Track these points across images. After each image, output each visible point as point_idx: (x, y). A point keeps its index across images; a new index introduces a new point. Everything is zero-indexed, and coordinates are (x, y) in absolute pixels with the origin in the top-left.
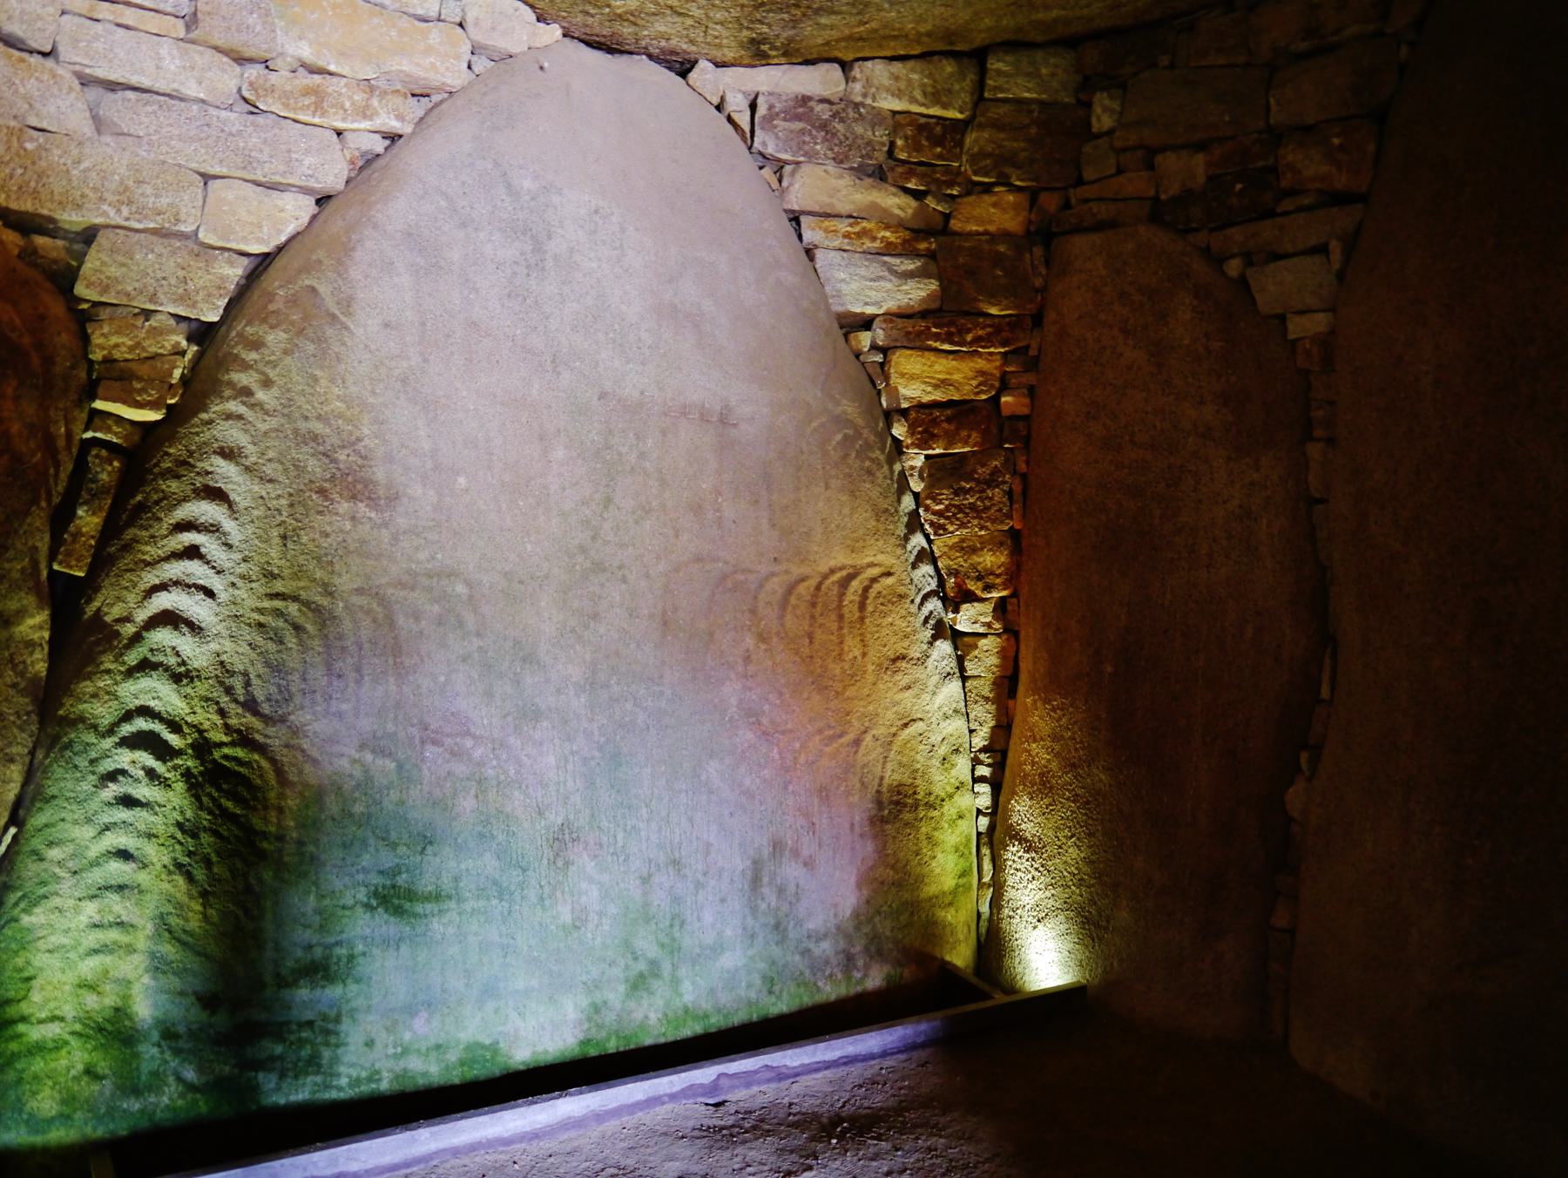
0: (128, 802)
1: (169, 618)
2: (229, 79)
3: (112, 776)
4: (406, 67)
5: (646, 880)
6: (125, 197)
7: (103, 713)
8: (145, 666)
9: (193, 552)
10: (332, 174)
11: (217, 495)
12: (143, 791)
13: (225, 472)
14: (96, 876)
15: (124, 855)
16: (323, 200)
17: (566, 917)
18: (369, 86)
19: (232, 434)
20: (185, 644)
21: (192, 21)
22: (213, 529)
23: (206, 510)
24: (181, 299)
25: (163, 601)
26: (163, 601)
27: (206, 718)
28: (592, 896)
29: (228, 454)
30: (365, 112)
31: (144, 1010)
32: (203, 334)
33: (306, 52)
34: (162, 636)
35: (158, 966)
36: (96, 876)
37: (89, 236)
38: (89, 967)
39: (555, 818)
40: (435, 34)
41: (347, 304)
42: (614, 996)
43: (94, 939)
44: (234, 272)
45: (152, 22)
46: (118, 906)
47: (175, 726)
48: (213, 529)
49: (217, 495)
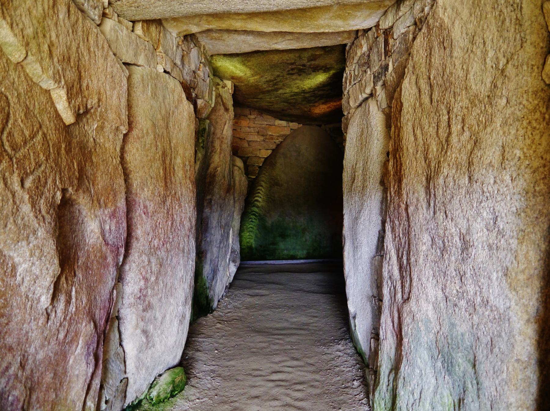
0: (252, 221)
1: (257, 201)
2: (262, 138)
3: (251, 218)
4: (282, 133)
5: (316, 236)
6: (252, 153)
7: (250, 211)
8: (254, 206)
9: (259, 193)
10: (274, 147)
11: (262, 186)
12: (254, 220)
13: (263, 183)
14: (249, 230)
15: (252, 228)
16: (273, 150)
17: (304, 240)
18: (278, 136)
19: (264, 179)
20: (258, 204)
21: (258, 133)
22: (261, 190)
23: (260, 188)
24: (258, 163)
25: (256, 198)
26: (256, 198)
27: (261, 212)
28: (308, 238)
29: (263, 181)
30: (278, 139)
31: (253, 246)
32: (260, 167)
33: (270, 133)
34: (256, 203)
35: (255, 240)
36: (249, 230)
37: (248, 157)
38: (248, 240)
39: (303, 227)
40: (286, 129)
41: (276, 163)
42: (311, 251)
43: (248, 237)
44: (263, 160)
45: (254, 134)
46: (251, 234)
47: (257, 213)
48: (261, 190)
49: (262, 186)
